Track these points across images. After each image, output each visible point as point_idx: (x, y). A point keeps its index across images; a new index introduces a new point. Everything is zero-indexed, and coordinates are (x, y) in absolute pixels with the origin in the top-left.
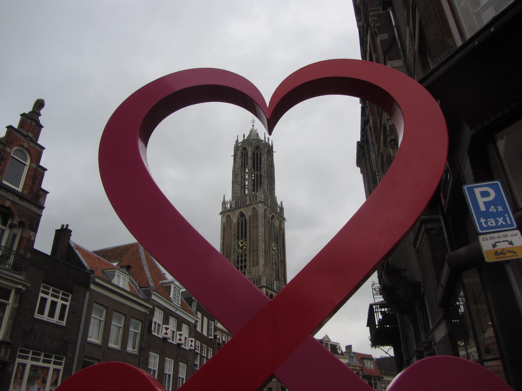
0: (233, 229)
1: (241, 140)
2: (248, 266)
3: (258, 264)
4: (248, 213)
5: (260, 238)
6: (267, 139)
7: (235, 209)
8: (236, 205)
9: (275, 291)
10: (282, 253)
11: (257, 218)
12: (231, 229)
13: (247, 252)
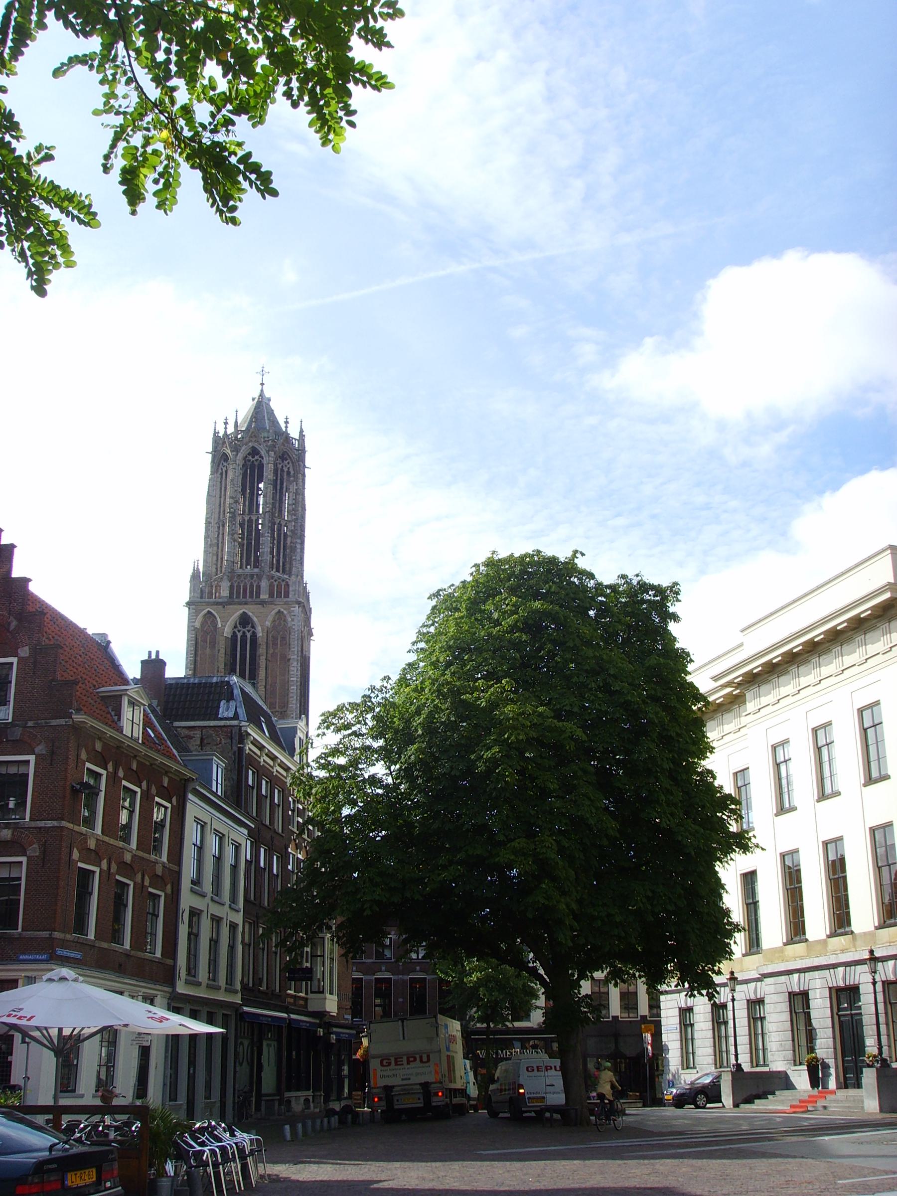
8: (231, 593)
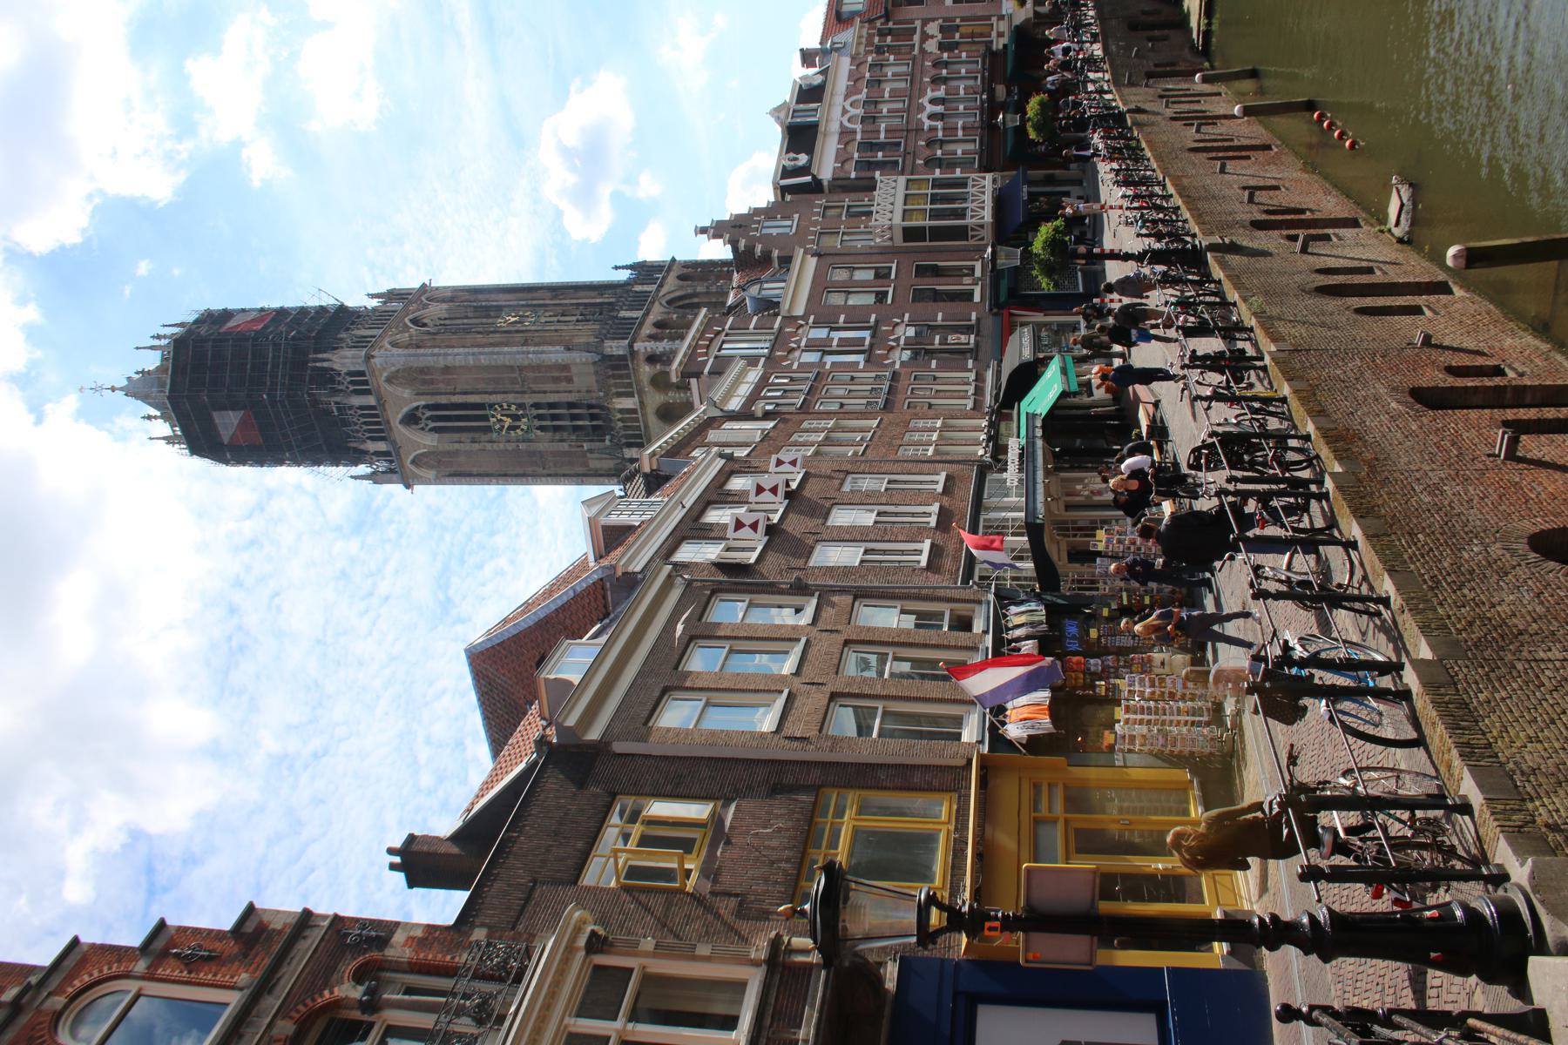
0: (457, 446)
1: (163, 428)
2: (571, 398)
3: (566, 367)
4: (403, 399)
5: (484, 360)
6: (157, 342)
7: (394, 443)
9: (647, 314)
10: (530, 295)
11: (422, 371)
12: (456, 453)
13: (529, 400)
